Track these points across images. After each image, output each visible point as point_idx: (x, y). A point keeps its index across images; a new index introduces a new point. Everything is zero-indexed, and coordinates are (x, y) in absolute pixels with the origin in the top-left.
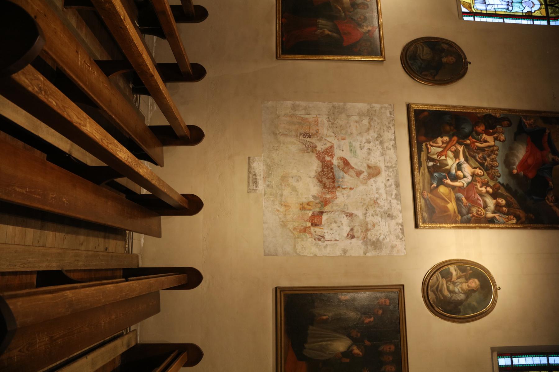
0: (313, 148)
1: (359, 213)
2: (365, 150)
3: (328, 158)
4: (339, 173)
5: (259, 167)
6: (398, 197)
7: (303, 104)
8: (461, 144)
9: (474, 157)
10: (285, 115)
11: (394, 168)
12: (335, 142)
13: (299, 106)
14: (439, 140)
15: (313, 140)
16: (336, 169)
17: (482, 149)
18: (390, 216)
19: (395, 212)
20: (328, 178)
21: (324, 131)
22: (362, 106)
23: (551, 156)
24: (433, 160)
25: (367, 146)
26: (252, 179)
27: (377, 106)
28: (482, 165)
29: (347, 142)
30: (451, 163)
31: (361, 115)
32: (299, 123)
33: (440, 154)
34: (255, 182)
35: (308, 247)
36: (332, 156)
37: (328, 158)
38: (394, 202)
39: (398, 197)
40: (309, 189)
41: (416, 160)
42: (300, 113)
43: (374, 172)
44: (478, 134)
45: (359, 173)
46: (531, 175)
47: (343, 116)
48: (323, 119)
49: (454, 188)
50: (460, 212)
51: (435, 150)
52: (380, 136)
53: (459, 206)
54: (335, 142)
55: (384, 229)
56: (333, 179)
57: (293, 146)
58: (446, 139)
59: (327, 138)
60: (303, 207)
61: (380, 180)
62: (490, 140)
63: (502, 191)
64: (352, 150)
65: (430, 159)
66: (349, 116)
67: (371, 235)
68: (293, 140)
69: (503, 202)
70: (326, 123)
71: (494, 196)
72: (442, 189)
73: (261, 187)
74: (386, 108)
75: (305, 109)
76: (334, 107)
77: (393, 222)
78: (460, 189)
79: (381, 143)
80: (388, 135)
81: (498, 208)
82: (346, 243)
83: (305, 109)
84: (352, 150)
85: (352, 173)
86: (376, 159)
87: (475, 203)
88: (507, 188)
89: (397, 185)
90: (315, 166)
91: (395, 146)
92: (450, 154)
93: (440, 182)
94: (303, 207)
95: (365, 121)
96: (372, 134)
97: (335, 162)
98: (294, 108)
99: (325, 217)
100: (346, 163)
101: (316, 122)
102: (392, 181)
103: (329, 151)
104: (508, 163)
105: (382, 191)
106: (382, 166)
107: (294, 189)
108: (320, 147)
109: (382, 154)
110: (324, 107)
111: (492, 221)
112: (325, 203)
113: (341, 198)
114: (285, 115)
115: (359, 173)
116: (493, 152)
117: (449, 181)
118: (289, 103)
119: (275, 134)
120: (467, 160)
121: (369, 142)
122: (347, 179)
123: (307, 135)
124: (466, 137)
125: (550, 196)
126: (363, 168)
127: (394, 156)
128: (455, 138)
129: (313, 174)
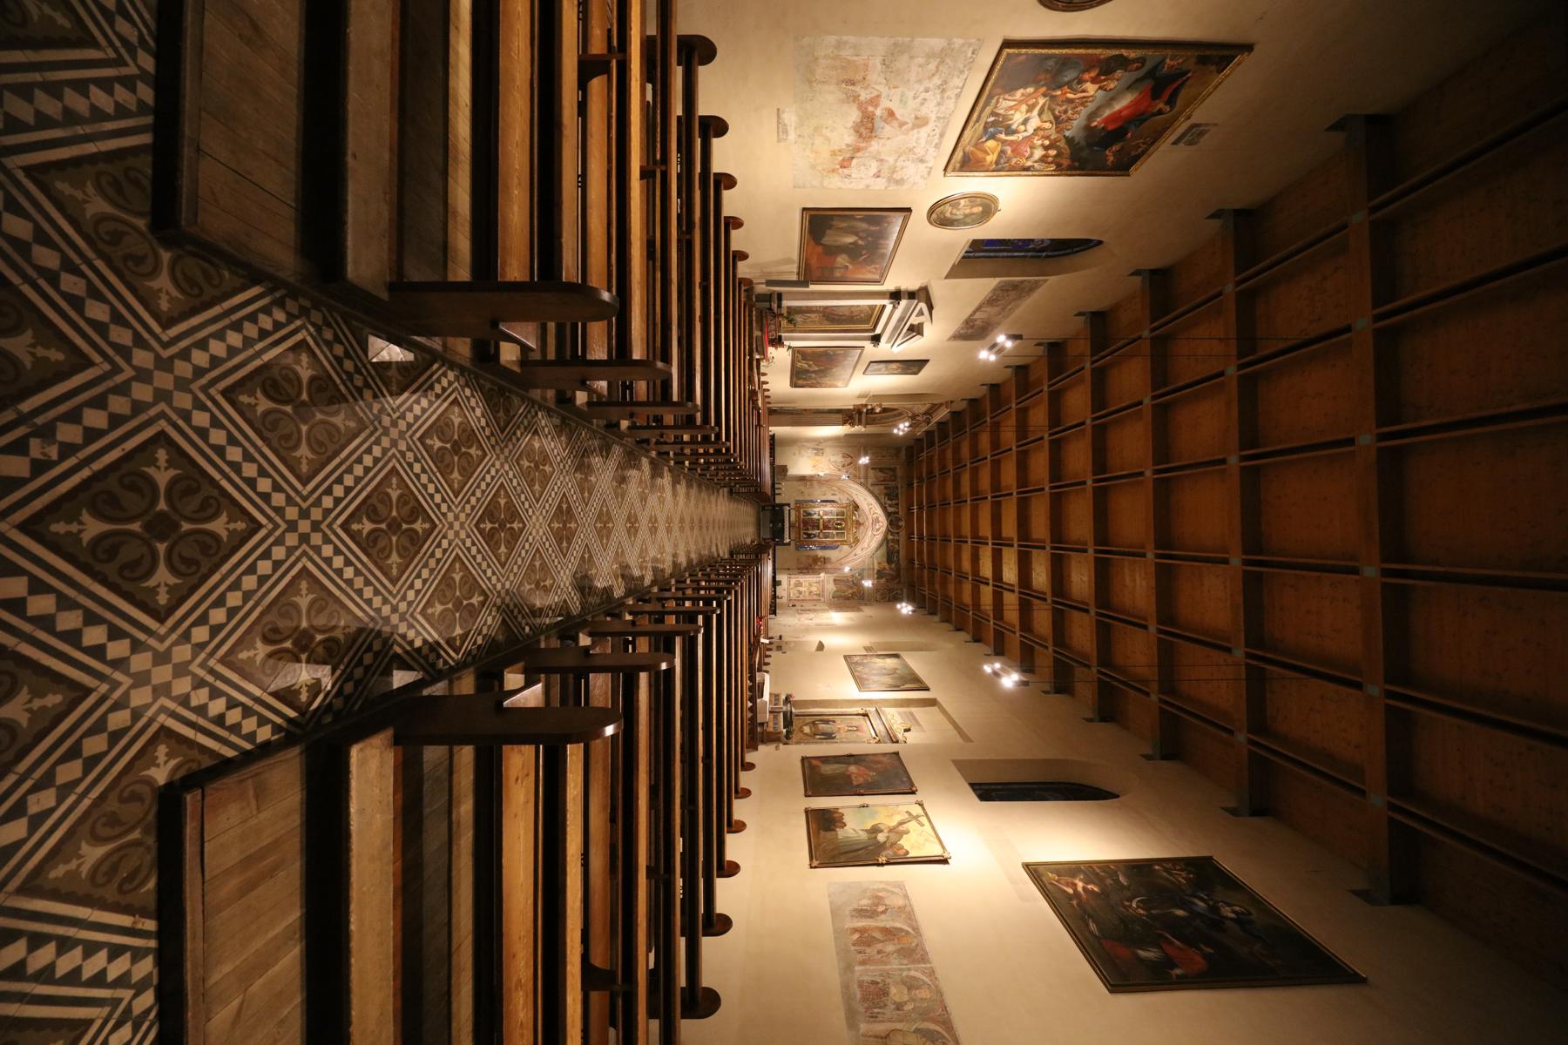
0: (856, 98)
1: (891, 160)
2: (919, 100)
3: (870, 109)
4: (878, 123)
5: (790, 118)
6: (937, 146)
7: (851, 39)
8: (1044, 95)
9: (1052, 111)
10: (825, 57)
11: (945, 120)
12: (884, 90)
13: (846, 43)
14: (1019, 94)
15: (857, 88)
16: (877, 120)
17: (1071, 101)
18: (922, 161)
19: (927, 158)
20: (867, 128)
21: (876, 77)
22: (937, 43)
23: (1161, 105)
24: (997, 115)
25: (924, 95)
26: (782, 129)
27: (958, 42)
28: (1056, 118)
29: (899, 91)
30: (1018, 117)
31: (930, 56)
32: (843, 68)
33: (1011, 108)
34: (786, 132)
35: (835, 182)
36: (876, 106)
37: (870, 109)
38: (932, 150)
39: (937, 146)
40: (842, 135)
41: (978, 109)
42: (846, 53)
43: (920, 122)
44: (1080, 82)
45: (902, 124)
46: (1111, 127)
47: (905, 57)
48: (877, 62)
49: (1004, 142)
50: (997, 163)
51: (1004, 104)
52: (945, 82)
53: (999, 157)
54: (884, 90)
55: (911, 171)
56: (872, 130)
57: (831, 95)
58: (1030, 90)
59: (877, 82)
60: (834, 153)
61: (924, 131)
62: (1091, 88)
63: (1062, 144)
64: (903, 101)
65: (993, 114)
66: (912, 58)
67: (897, 176)
68: (832, 88)
69: (1053, 152)
70: (879, 66)
71: (1046, 148)
72: (991, 144)
73: (792, 136)
74: (970, 45)
75: (855, 47)
76: (895, 45)
77: (922, 166)
78: (1011, 143)
79: (943, 91)
80: (957, 82)
81: (1043, 159)
82: (871, 181)
83: (855, 47)
84: (903, 101)
85: (895, 124)
86: (930, 110)
87: (1020, 155)
88: (1069, 141)
89: (942, 135)
90: (854, 115)
91: (958, 96)
92: (1024, 108)
93: (993, 137)
94: (834, 153)
95: (932, 66)
96: (937, 81)
97: (878, 112)
98: (839, 45)
99: (854, 161)
100: (891, 114)
101: (866, 66)
102: (938, 131)
103: (874, 101)
104: (1091, 116)
105: (923, 142)
106: (933, 117)
107: (828, 139)
108: (864, 95)
109: (939, 104)
110: (881, 44)
111: (1027, 169)
112: (858, 150)
113: (875, 146)
114: (825, 57)
115: (902, 124)
116: (1083, 104)
117: (1003, 136)
118: (832, 39)
119: (810, 82)
120: (1040, 114)
121: (927, 91)
122: (888, 130)
123: (850, 80)
124: (1059, 87)
125: (1115, 148)
126: (910, 120)
127: (952, 106)
128: (1043, 89)
129: (850, 124)
